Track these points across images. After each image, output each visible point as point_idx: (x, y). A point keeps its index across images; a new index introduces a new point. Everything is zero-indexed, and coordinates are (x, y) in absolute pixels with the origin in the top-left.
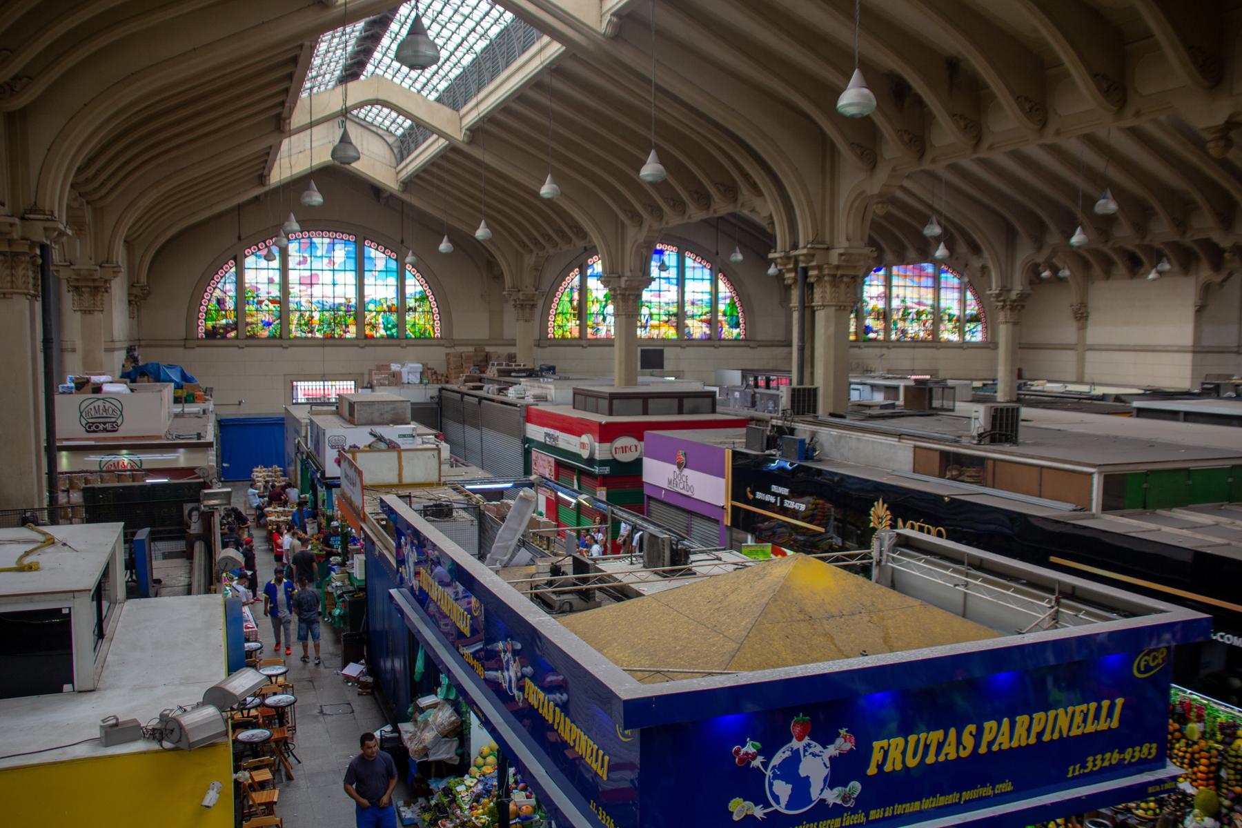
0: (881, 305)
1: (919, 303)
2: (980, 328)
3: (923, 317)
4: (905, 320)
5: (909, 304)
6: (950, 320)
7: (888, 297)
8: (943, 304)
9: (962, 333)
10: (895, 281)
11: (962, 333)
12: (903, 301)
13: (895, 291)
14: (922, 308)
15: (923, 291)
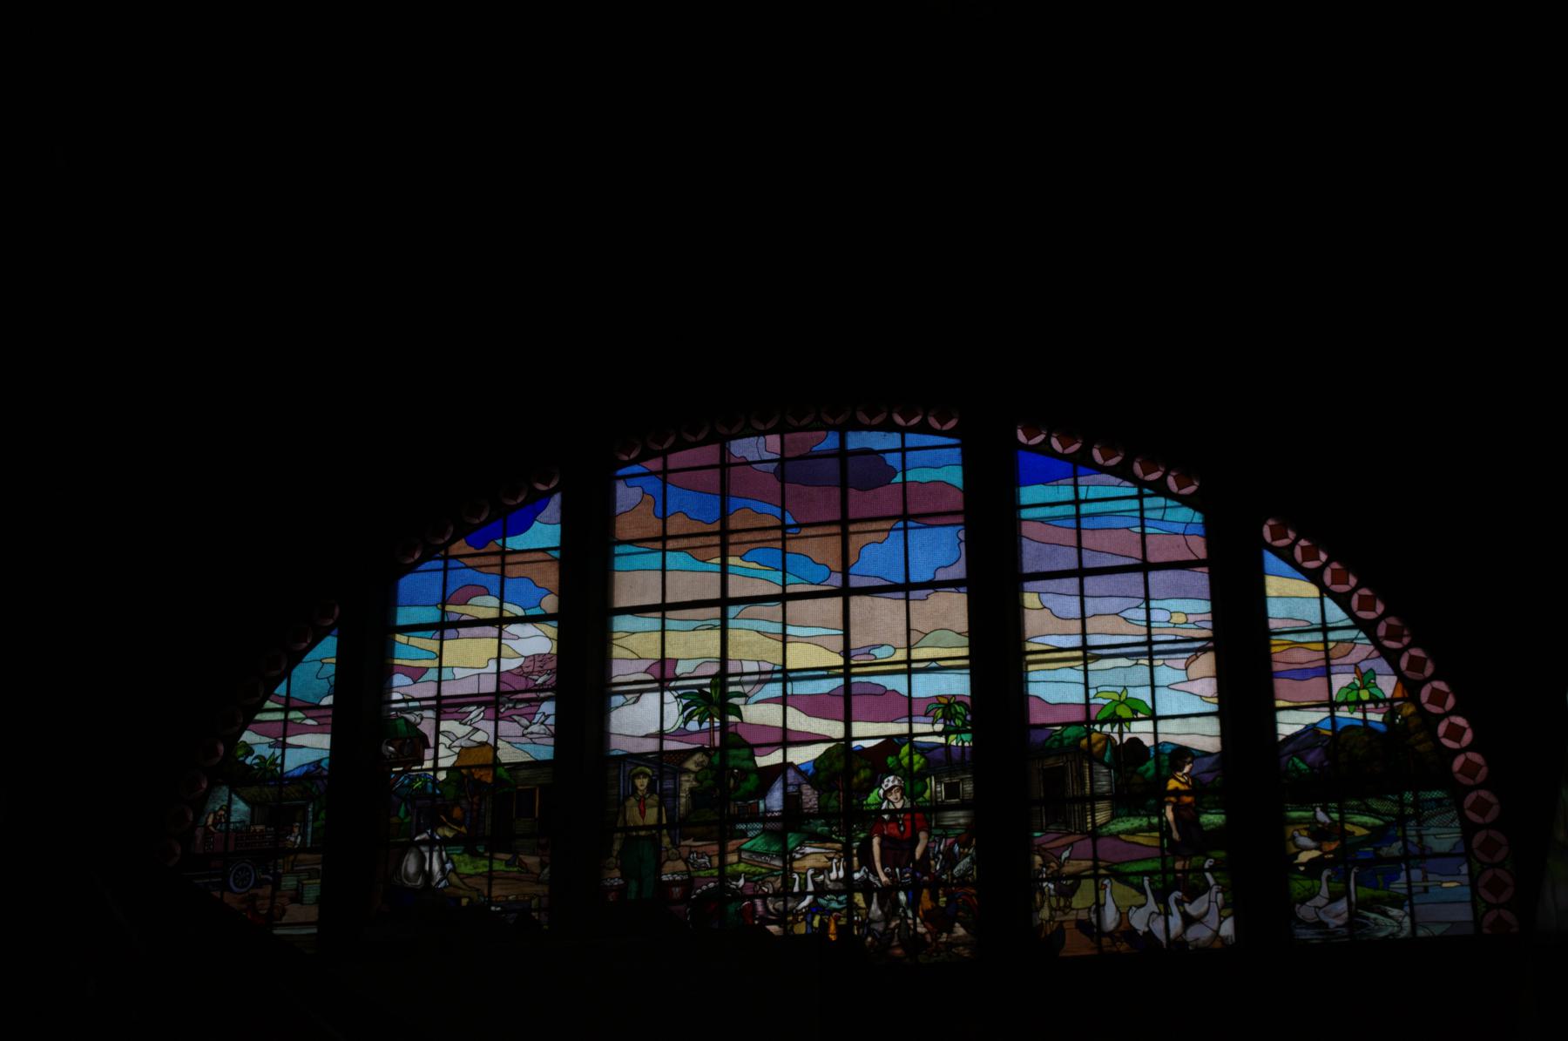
0: (525, 741)
1: (846, 706)
2: (1443, 837)
3: (888, 794)
4: (724, 832)
5: (760, 713)
6: (1128, 799)
7: (581, 680)
8: (1053, 688)
9: (1260, 883)
10: (634, 580)
11: (1260, 883)
12: (715, 696)
13: (633, 645)
14: (868, 732)
15: (880, 621)
